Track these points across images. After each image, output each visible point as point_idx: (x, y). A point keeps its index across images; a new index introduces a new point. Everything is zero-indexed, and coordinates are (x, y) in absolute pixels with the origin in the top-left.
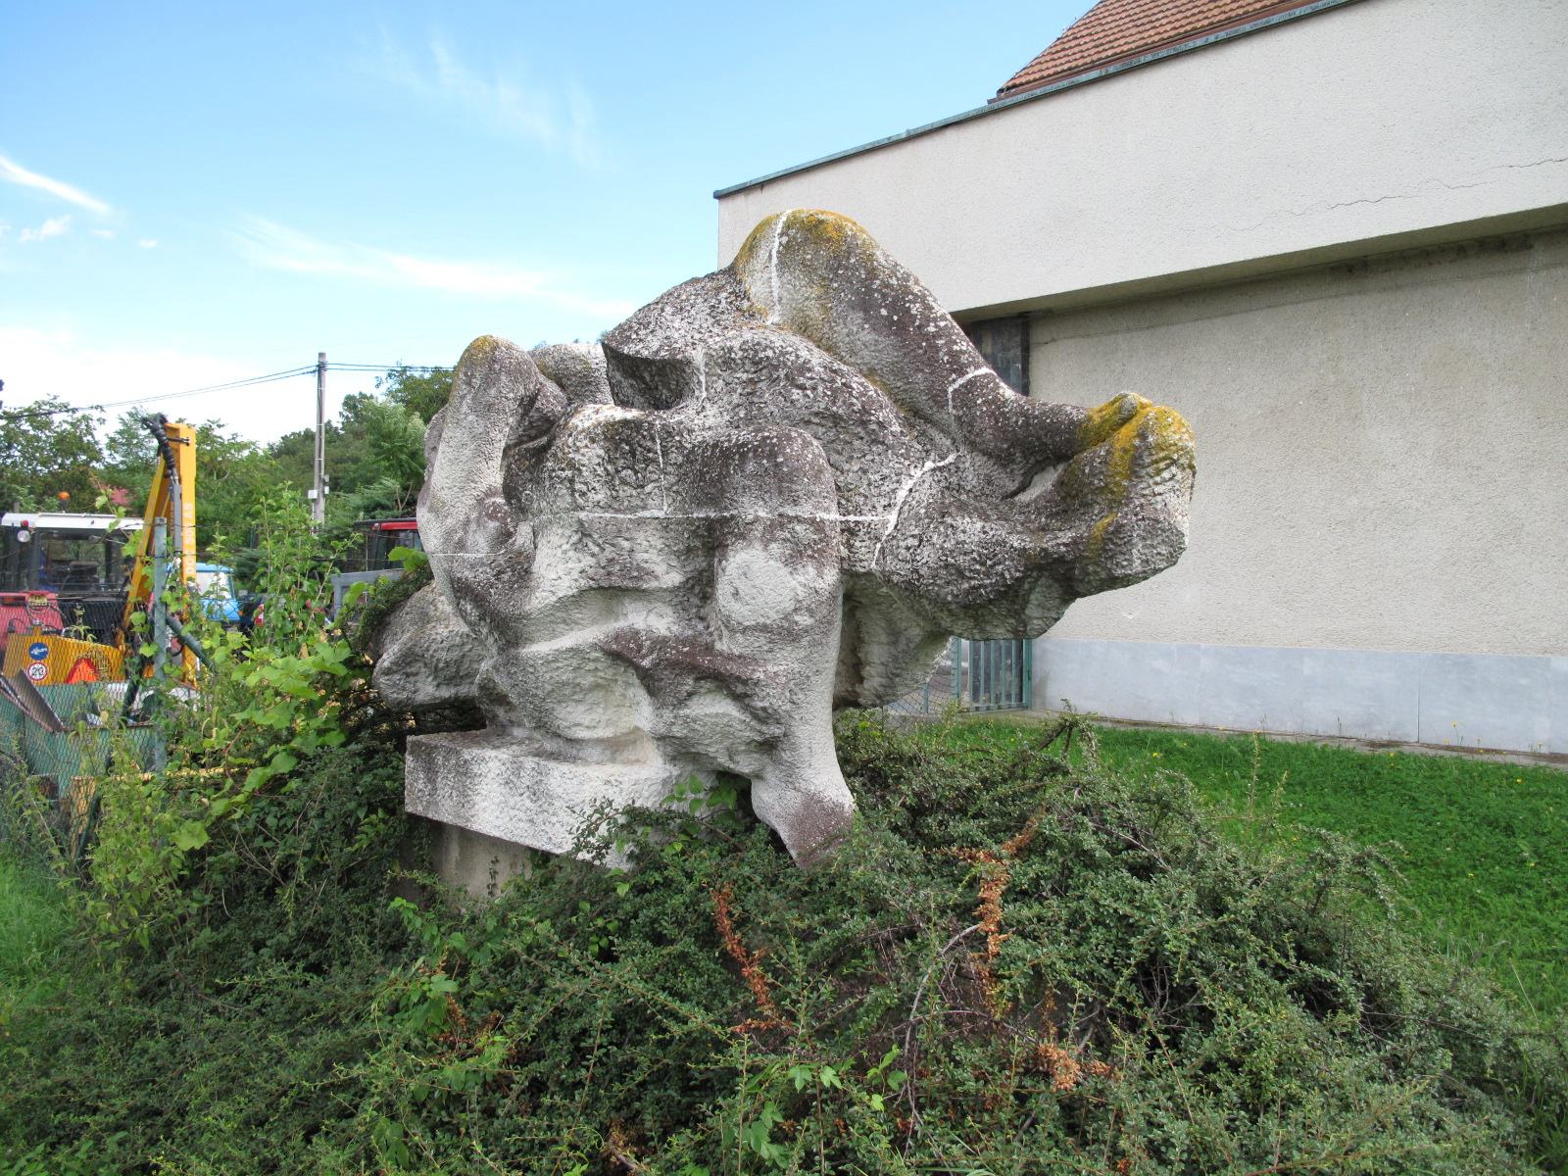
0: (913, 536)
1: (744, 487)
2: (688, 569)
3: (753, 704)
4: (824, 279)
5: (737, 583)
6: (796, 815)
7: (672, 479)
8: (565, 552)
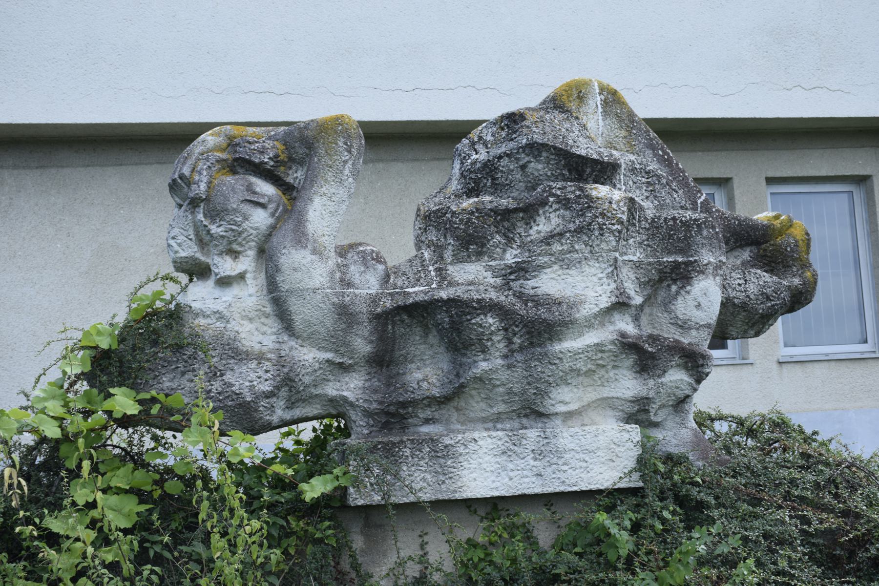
0: (739, 279)
1: (702, 244)
2: (645, 293)
3: (704, 370)
4: (628, 127)
5: (700, 300)
6: (692, 442)
7: (645, 238)
8: (600, 279)
